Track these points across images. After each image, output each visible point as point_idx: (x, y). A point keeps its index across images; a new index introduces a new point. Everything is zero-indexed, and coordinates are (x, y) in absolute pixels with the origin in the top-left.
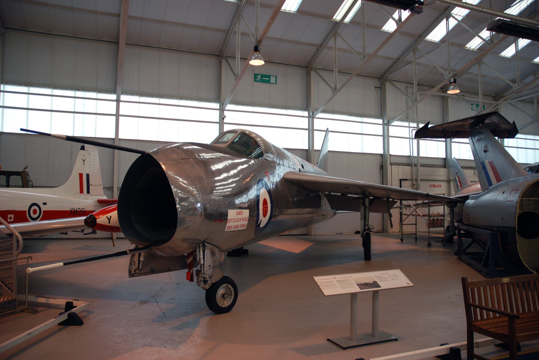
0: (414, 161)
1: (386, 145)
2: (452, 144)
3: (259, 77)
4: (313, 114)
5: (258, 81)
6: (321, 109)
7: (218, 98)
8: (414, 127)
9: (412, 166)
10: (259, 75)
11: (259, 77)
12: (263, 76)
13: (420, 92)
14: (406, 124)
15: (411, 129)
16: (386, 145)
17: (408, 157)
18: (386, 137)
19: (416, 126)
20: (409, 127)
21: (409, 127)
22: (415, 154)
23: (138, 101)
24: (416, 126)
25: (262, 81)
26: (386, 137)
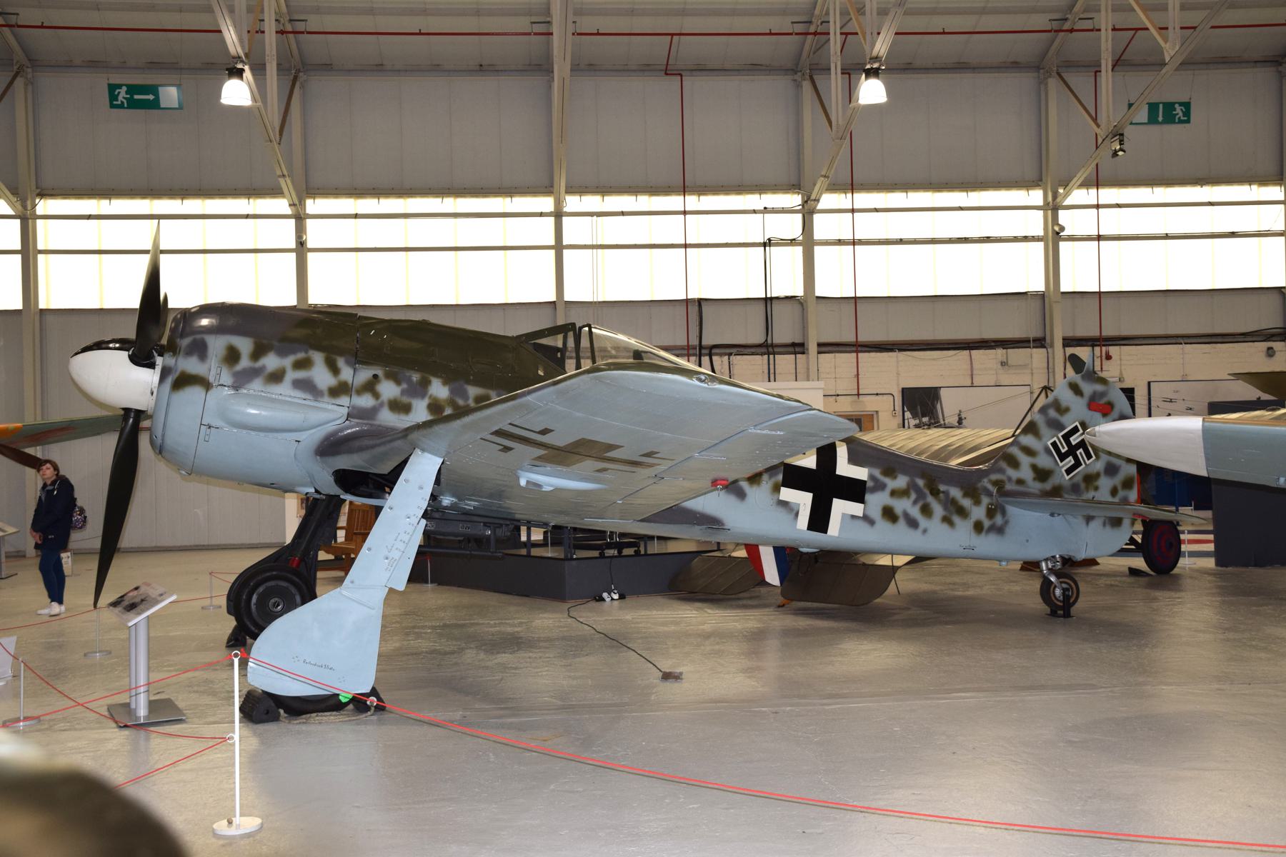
3: (122, 94)
5: (121, 106)
10: (120, 86)
11: (122, 94)
12: (132, 89)
25: (133, 104)
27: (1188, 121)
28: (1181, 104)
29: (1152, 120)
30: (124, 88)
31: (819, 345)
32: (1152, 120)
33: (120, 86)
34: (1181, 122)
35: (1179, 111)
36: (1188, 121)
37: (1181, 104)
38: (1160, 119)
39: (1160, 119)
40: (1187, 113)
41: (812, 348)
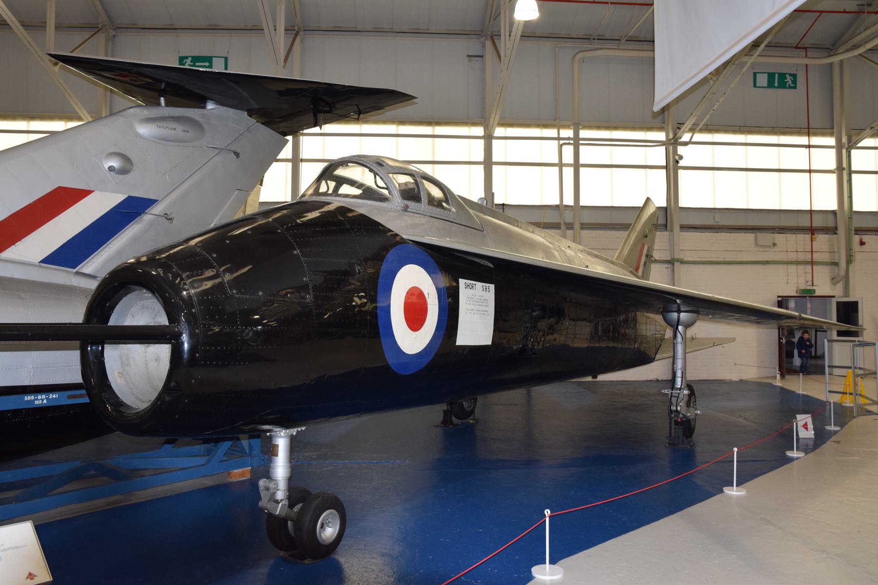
0: (569, 217)
1: (845, 190)
2: (680, 172)
4: (675, 135)
6: (689, 124)
7: (481, 118)
8: (569, 139)
9: (560, 228)
10: (187, 58)
13: (581, 55)
14: (553, 133)
15: (562, 142)
16: (845, 190)
17: (557, 207)
18: (844, 172)
19: (572, 136)
20: (559, 139)
21: (559, 139)
22: (569, 201)
23: (25, 129)
24: (572, 136)
26: (844, 172)
27: (795, 88)
28: (790, 75)
29: (770, 85)
30: (190, 59)
31: (582, 224)
32: (770, 85)
33: (187, 58)
34: (790, 87)
35: (789, 79)
36: (795, 88)
37: (790, 75)
38: (776, 84)
39: (776, 84)
40: (794, 81)
41: (577, 226)
